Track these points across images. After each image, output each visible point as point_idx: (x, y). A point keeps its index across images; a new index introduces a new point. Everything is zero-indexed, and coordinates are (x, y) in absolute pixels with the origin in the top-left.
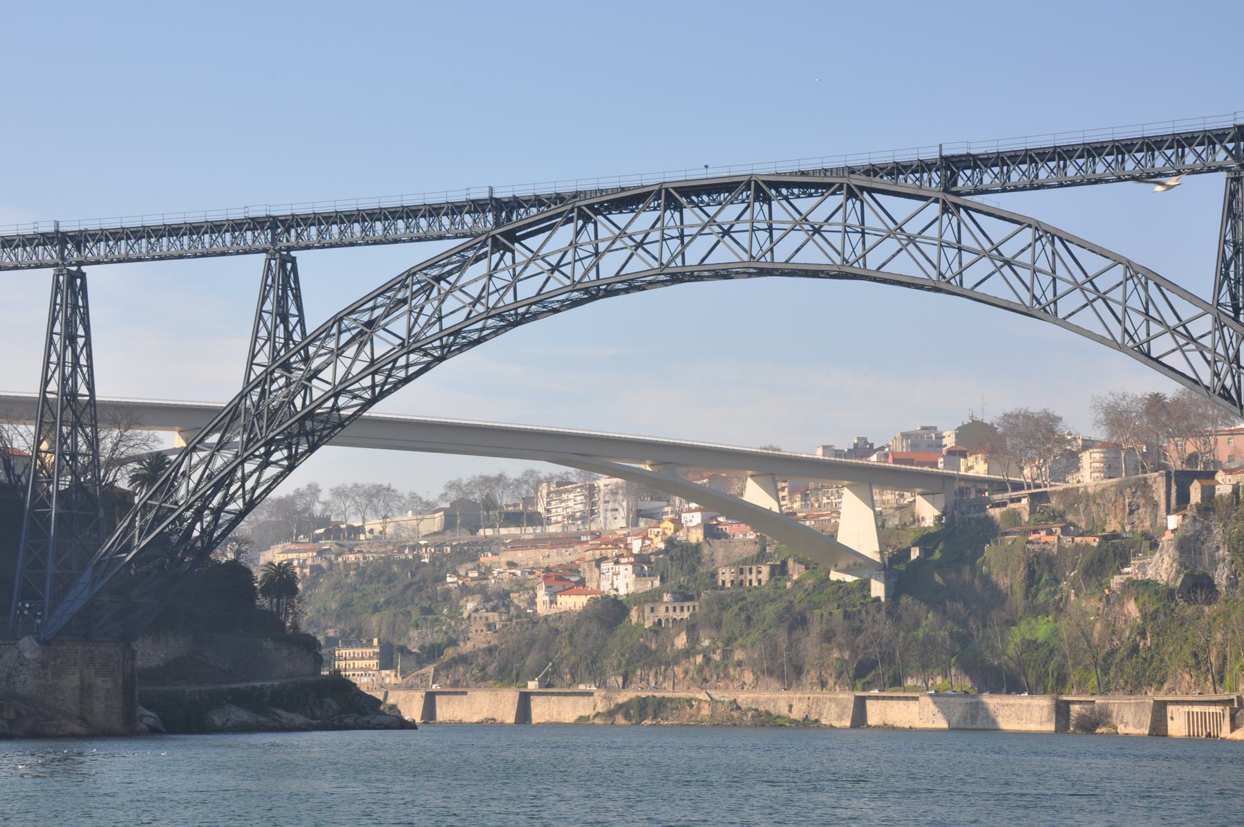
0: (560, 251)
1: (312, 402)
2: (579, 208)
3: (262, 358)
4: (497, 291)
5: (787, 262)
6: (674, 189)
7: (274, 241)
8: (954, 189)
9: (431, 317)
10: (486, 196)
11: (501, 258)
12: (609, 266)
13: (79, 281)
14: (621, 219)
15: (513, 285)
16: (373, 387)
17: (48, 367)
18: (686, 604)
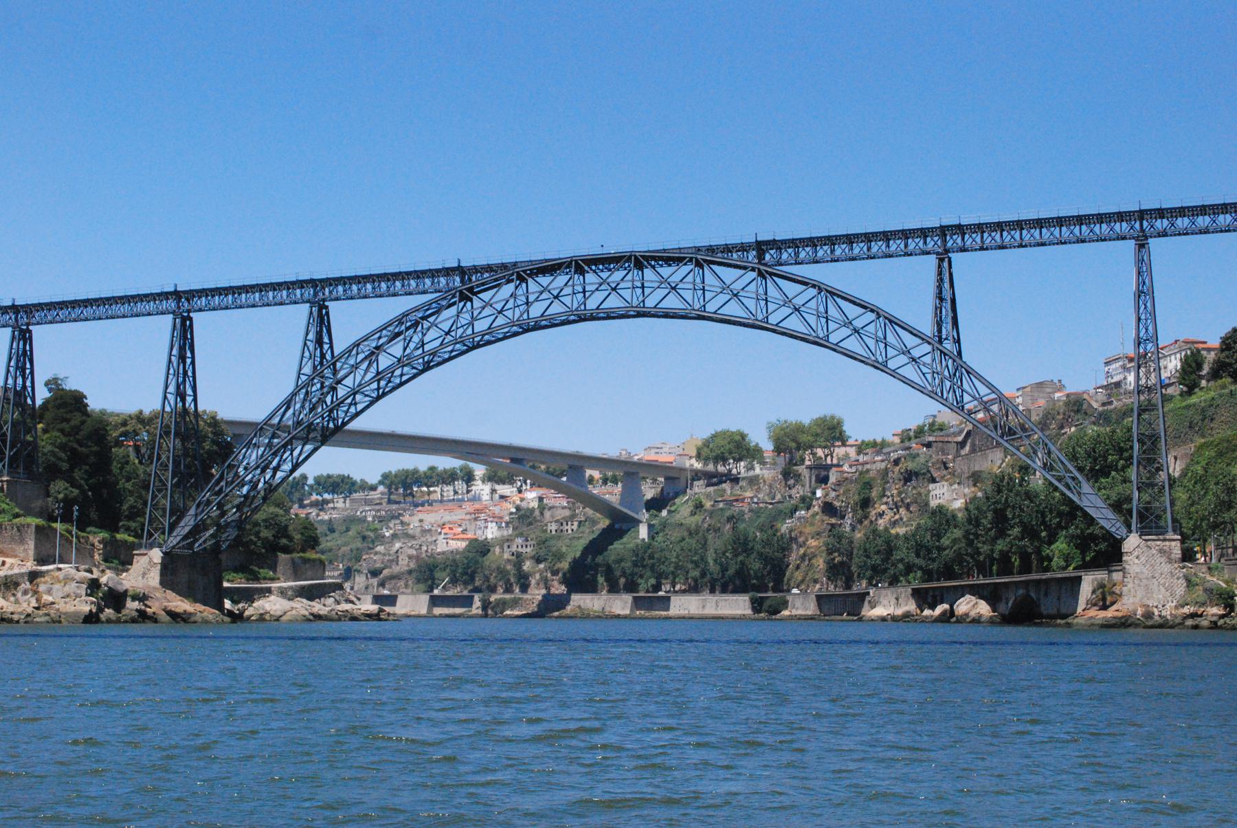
0: (504, 300)
1: (337, 399)
2: (518, 272)
3: (307, 370)
4: (462, 326)
5: (655, 307)
6: (581, 260)
7: (316, 294)
8: (763, 262)
9: (418, 344)
10: (456, 265)
11: (464, 305)
12: (536, 311)
13: (188, 323)
14: (544, 280)
15: (471, 324)
16: (378, 389)
17: (168, 377)
18: (528, 543)
